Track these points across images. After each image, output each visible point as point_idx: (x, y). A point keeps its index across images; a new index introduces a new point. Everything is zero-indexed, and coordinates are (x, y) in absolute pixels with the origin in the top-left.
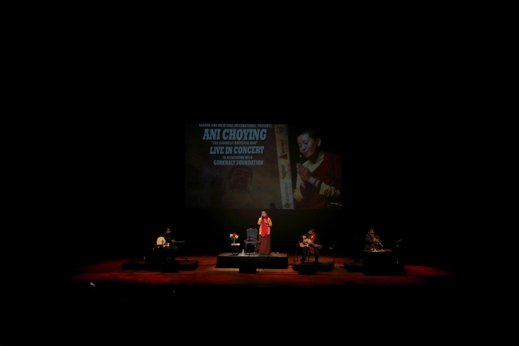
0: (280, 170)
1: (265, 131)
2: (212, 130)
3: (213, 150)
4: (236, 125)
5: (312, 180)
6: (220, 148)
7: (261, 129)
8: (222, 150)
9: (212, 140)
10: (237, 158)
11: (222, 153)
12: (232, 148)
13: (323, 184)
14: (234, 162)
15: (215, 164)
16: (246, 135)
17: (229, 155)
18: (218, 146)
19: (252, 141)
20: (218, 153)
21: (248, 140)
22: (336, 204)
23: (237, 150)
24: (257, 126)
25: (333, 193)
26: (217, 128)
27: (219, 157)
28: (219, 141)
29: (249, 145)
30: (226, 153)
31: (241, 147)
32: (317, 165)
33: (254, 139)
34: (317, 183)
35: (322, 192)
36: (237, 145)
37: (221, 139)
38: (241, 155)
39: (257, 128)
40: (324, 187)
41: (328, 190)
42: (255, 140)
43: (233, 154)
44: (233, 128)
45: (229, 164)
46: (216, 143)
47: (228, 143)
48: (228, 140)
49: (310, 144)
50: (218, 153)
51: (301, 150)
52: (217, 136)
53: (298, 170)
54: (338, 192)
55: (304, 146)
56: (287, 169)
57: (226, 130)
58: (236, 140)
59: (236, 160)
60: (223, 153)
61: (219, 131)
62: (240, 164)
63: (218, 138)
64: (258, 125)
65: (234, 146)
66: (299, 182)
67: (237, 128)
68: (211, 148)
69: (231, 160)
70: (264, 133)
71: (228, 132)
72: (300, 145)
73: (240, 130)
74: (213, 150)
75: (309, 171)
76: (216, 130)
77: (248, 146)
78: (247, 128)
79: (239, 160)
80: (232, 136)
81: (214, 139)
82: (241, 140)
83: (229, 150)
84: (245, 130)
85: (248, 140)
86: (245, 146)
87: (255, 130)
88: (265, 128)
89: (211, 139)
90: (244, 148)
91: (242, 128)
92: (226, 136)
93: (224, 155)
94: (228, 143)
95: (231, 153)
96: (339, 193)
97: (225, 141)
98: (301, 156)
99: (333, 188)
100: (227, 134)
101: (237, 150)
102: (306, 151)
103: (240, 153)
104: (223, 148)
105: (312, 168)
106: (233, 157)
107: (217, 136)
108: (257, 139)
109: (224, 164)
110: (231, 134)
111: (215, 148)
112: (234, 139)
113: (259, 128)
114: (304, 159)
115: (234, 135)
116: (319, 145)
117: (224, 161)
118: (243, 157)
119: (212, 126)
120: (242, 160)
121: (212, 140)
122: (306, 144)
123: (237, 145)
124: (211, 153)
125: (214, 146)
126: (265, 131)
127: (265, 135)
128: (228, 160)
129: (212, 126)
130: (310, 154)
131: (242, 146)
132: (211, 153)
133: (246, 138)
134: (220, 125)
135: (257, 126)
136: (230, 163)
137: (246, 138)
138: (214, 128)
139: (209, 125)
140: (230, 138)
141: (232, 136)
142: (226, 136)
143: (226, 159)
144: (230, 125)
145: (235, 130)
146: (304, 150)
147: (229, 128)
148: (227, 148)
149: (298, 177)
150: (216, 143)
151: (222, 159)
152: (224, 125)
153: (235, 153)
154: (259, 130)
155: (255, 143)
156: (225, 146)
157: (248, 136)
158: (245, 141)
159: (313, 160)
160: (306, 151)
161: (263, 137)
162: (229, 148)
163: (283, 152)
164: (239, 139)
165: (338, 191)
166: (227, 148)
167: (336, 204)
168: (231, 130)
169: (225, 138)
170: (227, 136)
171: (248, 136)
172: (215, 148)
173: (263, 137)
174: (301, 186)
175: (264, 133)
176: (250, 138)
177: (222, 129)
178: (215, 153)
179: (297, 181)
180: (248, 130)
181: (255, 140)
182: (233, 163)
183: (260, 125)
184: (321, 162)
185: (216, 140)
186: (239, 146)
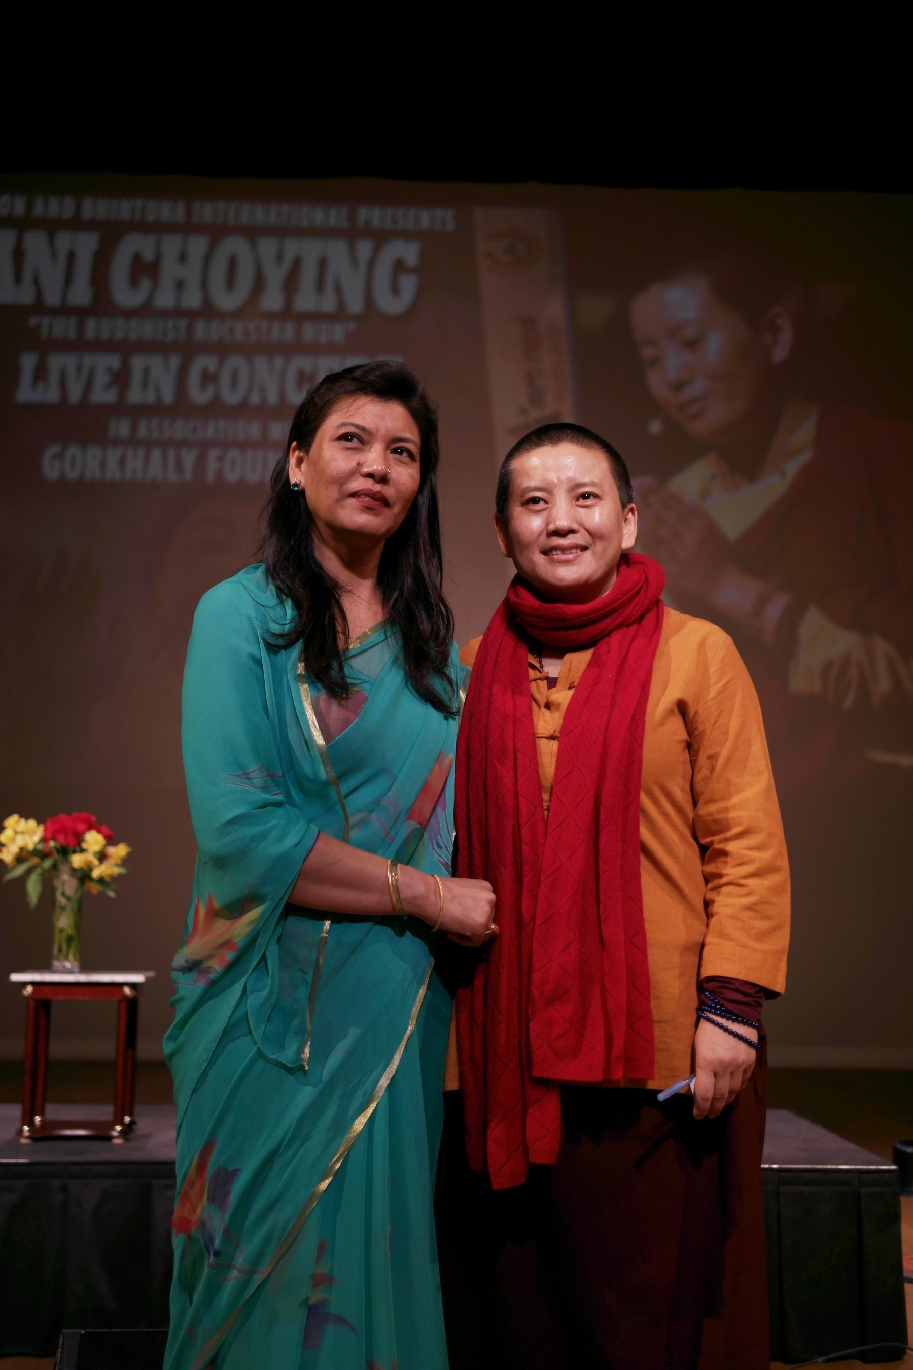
1: (410, 253)
2: (35, 242)
3: (40, 373)
4: (207, 212)
6: (88, 360)
7: (380, 238)
8: (102, 378)
9: (39, 306)
10: (211, 430)
11: (103, 395)
12: (175, 361)
13: (813, 621)
14: (189, 458)
15: (50, 469)
16: (275, 277)
17: (156, 410)
18: (80, 345)
19: (316, 317)
20: (75, 395)
21: (287, 314)
23: (208, 378)
24: (352, 217)
25: (883, 684)
26: (76, 224)
27: (81, 423)
28: (81, 313)
29: (298, 347)
30: (135, 396)
31: (236, 361)
32: (770, 488)
33: (328, 304)
34: (774, 611)
35: (804, 676)
36: (208, 348)
37: (102, 304)
38: (242, 410)
39: (351, 235)
42: (340, 314)
43: (181, 407)
44: (186, 228)
45: (155, 469)
46: (63, 328)
47: (147, 329)
48: (145, 311)
49: (714, 346)
50: (75, 395)
51: (658, 383)
52: (68, 280)
55: (674, 361)
57: (133, 245)
58: (208, 311)
59: (204, 447)
60: (110, 397)
61: (87, 244)
62: (232, 477)
63: (81, 295)
64: (363, 213)
65: (188, 350)
67: (217, 233)
68: (28, 362)
69: (165, 445)
70: (399, 267)
71: (148, 256)
72: (647, 353)
73: (234, 245)
74: (40, 373)
75: (712, 532)
76: (64, 240)
77: (288, 350)
78: (282, 232)
79: (225, 445)
80: (180, 285)
81: (52, 298)
82: (237, 314)
83: (156, 377)
84: (268, 247)
85: (287, 314)
86: (270, 349)
87: (337, 250)
88: (406, 235)
89: (26, 296)
90: (260, 363)
91: (252, 233)
92: (134, 282)
93: (120, 408)
94: (147, 329)
95: (168, 397)
97: (129, 314)
98: (655, 427)
99: (881, 646)
100: (145, 270)
101: (208, 378)
102: (691, 392)
103: (231, 398)
104: (114, 361)
105: (738, 509)
106: (180, 429)
107: (68, 280)
108: (355, 305)
109: (112, 471)
110: (170, 270)
111: (56, 362)
112: (192, 300)
113: (368, 232)
114: (681, 449)
115: (192, 273)
116: (780, 354)
117: (113, 456)
118: (254, 430)
119: (38, 209)
120: (244, 445)
121: (39, 306)
122: (692, 345)
123: (208, 348)
124: (26, 394)
125: (47, 347)
126: (410, 253)
127: (409, 284)
128: (148, 445)
129: (38, 209)
130: (716, 415)
131: (249, 350)
132: (26, 394)
133: (273, 300)
134: (96, 208)
135: (352, 217)
136: (156, 467)
137: (273, 300)
138: (52, 227)
139: (19, 206)
140: (165, 299)
141: (180, 285)
142: (134, 282)
143: (132, 441)
144: (167, 210)
145: (198, 245)
146: (678, 386)
147: (159, 228)
148: (138, 363)
150: (63, 328)
151: (104, 440)
152: (125, 209)
153: (199, 396)
154: (364, 248)
155: (338, 332)
156: (126, 348)
157: (291, 284)
158: (271, 316)
159: (743, 457)
160: (691, 392)
161: (395, 290)
162: (156, 362)
163: (536, 397)
164: (226, 302)
166: (138, 363)
168: (171, 244)
169: (125, 296)
170: (145, 284)
171: (291, 284)
172: (56, 362)
173: (395, 290)
175: (399, 267)
176: (306, 300)
177: (111, 233)
178: (52, 395)
180: (292, 247)
181: (340, 314)
182: (179, 467)
183: (373, 215)
184: (793, 468)
185: (64, 310)
186: (222, 350)
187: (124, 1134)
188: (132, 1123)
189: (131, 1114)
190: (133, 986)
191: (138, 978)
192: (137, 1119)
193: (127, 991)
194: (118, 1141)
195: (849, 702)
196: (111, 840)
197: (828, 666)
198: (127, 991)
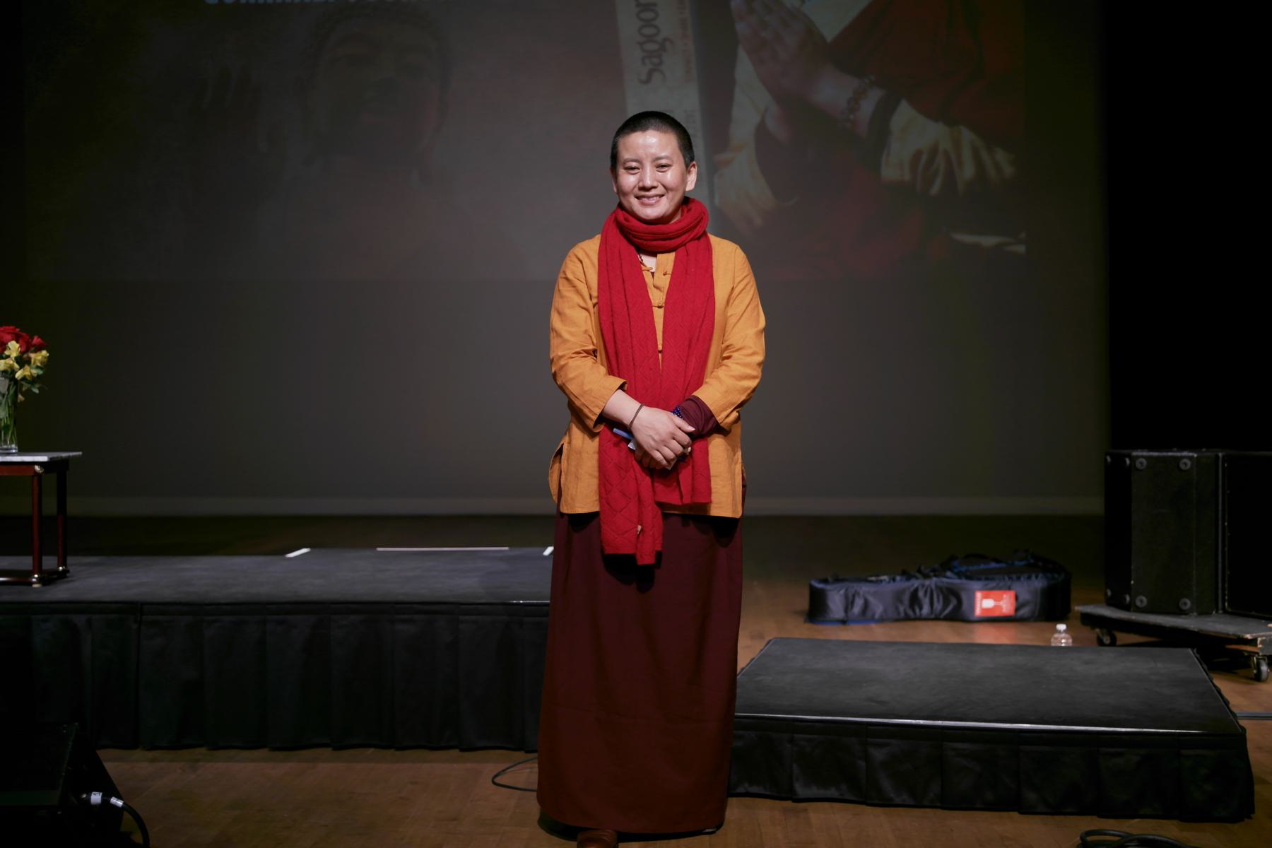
0: (628, 25)
5: (832, 91)
13: (905, 113)
22: (989, 241)
25: (968, 171)
34: (867, 107)
35: (895, 166)
40: (914, 134)
41: (934, 151)
53: (740, 27)
54: (1002, 163)
56: (671, 21)
66: (751, 106)
75: (811, 32)
96: (1008, 170)
99: (967, 136)
149: (745, 69)
165: (1001, 156)
167: (989, 241)
174: (762, 133)
179: (739, 96)
187: (39, 580)
188: (65, 572)
189: (64, 563)
190: (40, 464)
191: (43, 458)
192: (71, 569)
193: (37, 468)
194: (35, 586)
195: (935, 189)
196: (27, 348)
197: (918, 155)
198: (37, 468)
